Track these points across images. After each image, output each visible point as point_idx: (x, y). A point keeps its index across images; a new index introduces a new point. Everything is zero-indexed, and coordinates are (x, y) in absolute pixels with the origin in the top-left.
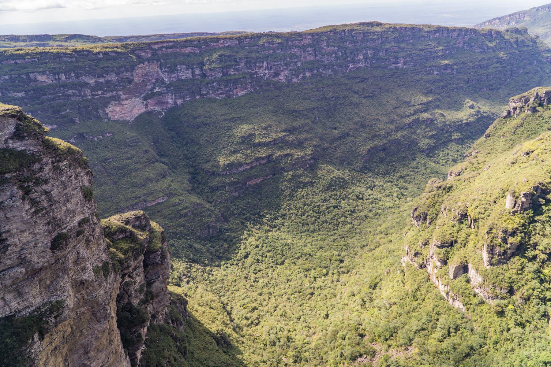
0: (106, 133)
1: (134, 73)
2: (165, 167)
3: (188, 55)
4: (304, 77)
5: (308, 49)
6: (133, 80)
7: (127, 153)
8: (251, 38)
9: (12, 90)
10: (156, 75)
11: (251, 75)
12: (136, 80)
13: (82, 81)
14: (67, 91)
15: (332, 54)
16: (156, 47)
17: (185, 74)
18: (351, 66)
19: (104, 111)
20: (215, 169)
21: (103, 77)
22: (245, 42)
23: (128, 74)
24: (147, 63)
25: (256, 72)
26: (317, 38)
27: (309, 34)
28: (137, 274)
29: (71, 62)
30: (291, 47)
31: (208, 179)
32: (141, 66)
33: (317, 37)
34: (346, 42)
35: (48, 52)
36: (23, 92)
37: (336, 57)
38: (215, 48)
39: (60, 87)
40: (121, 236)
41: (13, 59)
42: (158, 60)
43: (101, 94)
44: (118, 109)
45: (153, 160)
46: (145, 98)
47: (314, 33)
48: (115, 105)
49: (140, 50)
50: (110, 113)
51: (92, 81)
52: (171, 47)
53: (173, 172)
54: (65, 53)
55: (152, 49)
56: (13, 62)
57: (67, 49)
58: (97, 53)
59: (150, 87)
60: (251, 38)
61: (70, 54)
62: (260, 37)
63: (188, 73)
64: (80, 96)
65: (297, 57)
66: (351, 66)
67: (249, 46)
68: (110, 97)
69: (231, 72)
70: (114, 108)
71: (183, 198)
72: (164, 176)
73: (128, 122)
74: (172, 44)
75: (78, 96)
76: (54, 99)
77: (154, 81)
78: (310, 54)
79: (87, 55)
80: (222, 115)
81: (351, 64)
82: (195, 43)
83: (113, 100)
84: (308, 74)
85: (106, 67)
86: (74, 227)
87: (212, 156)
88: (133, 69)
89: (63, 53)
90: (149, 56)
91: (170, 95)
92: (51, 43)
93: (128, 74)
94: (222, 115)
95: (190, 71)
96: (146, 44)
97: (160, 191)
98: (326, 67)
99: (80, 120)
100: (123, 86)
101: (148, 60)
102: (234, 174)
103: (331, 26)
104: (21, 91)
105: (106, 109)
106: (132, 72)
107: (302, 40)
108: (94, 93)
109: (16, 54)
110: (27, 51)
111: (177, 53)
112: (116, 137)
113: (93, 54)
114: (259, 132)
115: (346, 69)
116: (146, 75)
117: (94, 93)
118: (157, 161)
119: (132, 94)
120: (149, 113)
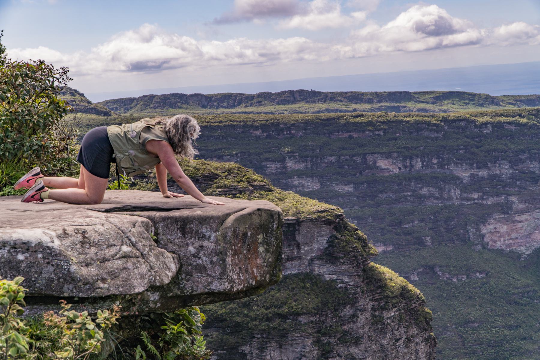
0: (475, 272)
7: (509, 315)
9: (337, 180)
13: (448, 172)
14: (421, 188)
19: (478, 229)
21: (486, 167)
29: (436, 139)
35: (402, 121)
36: (352, 185)
43: (478, 199)
44: (504, 228)
48: (500, 221)
50: (488, 235)
51: (465, 174)
54: (429, 123)
56: (346, 135)
57: (433, 116)
58: (483, 124)
61: (437, 125)
64: (441, 198)
68: (493, 205)
70: (497, 226)
73: (519, 256)
75: (437, 198)
76: (397, 200)
79: (464, 128)
85: (494, 150)
89: (425, 122)
92: (410, 105)
99: (433, 243)
100: (520, 187)
104: (348, 183)
108: (465, 195)
109: (354, 123)
110: (370, 119)
112: (492, 282)
117: (465, 195)
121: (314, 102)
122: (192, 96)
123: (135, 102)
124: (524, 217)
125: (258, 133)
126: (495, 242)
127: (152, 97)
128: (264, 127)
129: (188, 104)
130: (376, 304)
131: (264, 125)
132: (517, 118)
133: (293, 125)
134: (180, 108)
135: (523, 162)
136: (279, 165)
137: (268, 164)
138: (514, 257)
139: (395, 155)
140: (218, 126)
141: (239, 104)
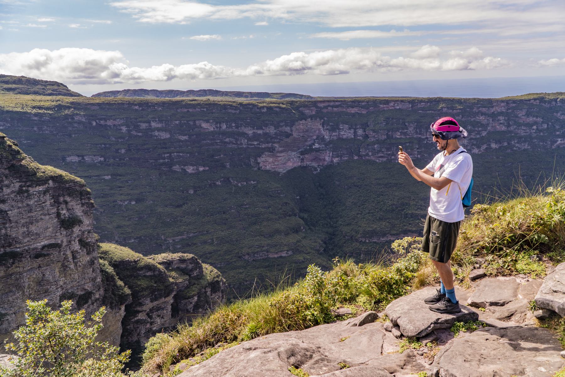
0: (250, 181)
1: (294, 128)
2: (302, 222)
3: (353, 115)
4: (489, 149)
5: (499, 117)
6: (291, 135)
7: (266, 202)
8: (428, 102)
9: (178, 133)
10: (317, 131)
11: (420, 140)
12: (295, 135)
13: (241, 131)
14: (225, 139)
15: (533, 126)
16: (322, 105)
17: (346, 133)
18: (559, 141)
19: (256, 160)
20: (354, 233)
21: (262, 129)
22: (419, 106)
23: (287, 129)
24: (309, 120)
25: (427, 138)
26: (513, 106)
27: (502, 101)
28: (159, 316)
30: (477, 114)
31: (345, 243)
32: (303, 121)
33: (514, 105)
34: (557, 112)
35: (217, 104)
37: (537, 129)
38: (384, 110)
39: (219, 134)
40: (149, 274)
42: (321, 118)
44: (271, 160)
45: (291, 213)
46: (302, 153)
47: (510, 100)
48: (269, 156)
51: (250, 132)
52: (337, 107)
53: (310, 229)
54: (231, 106)
55: (317, 107)
56: (186, 110)
58: (261, 107)
59: (310, 143)
60: (428, 102)
61: (236, 107)
63: (350, 133)
64: (237, 144)
65: (482, 125)
66: (559, 142)
67: (423, 110)
69: (398, 135)
70: (267, 158)
71: (309, 257)
72: (296, 230)
73: (279, 173)
75: (234, 144)
76: (212, 144)
77: (315, 137)
78: (501, 124)
80: (376, 179)
81: (559, 139)
82: (363, 104)
83: (267, 151)
84: (494, 146)
86: (36, 248)
87: (354, 219)
88: (294, 125)
89: (229, 105)
90: (314, 113)
91: (328, 152)
92: (268, 100)
93: (287, 129)
94: (376, 179)
95: (352, 131)
96: (312, 102)
97: (285, 245)
98: (520, 139)
99: (230, 166)
100: (280, 139)
101: (311, 117)
102: (375, 242)
103: (537, 94)
104: (185, 135)
105: (259, 159)
106: (291, 126)
107: (493, 107)
109: (190, 104)
111: (342, 112)
112: (259, 186)
113: (258, 108)
114: (415, 203)
115: (552, 145)
116: (307, 131)
118: (295, 215)
119: (288, 148)
120: (304, 168)
121: (216, 96)
122: (151, 90)
124: (282, 154)
125: (137, 107)
126: (266, 166)
127: (129, 90)
128: (141, 104)
129: (148, 94)
130: (23, 184)
131: (140, 103)
132: (281, 105)
133: (156, 104)
135: (282, 126)
136: (147, 125)
137: (141, 124)
138: (277, 174)
139: (211, 121)
141: (177, 96)
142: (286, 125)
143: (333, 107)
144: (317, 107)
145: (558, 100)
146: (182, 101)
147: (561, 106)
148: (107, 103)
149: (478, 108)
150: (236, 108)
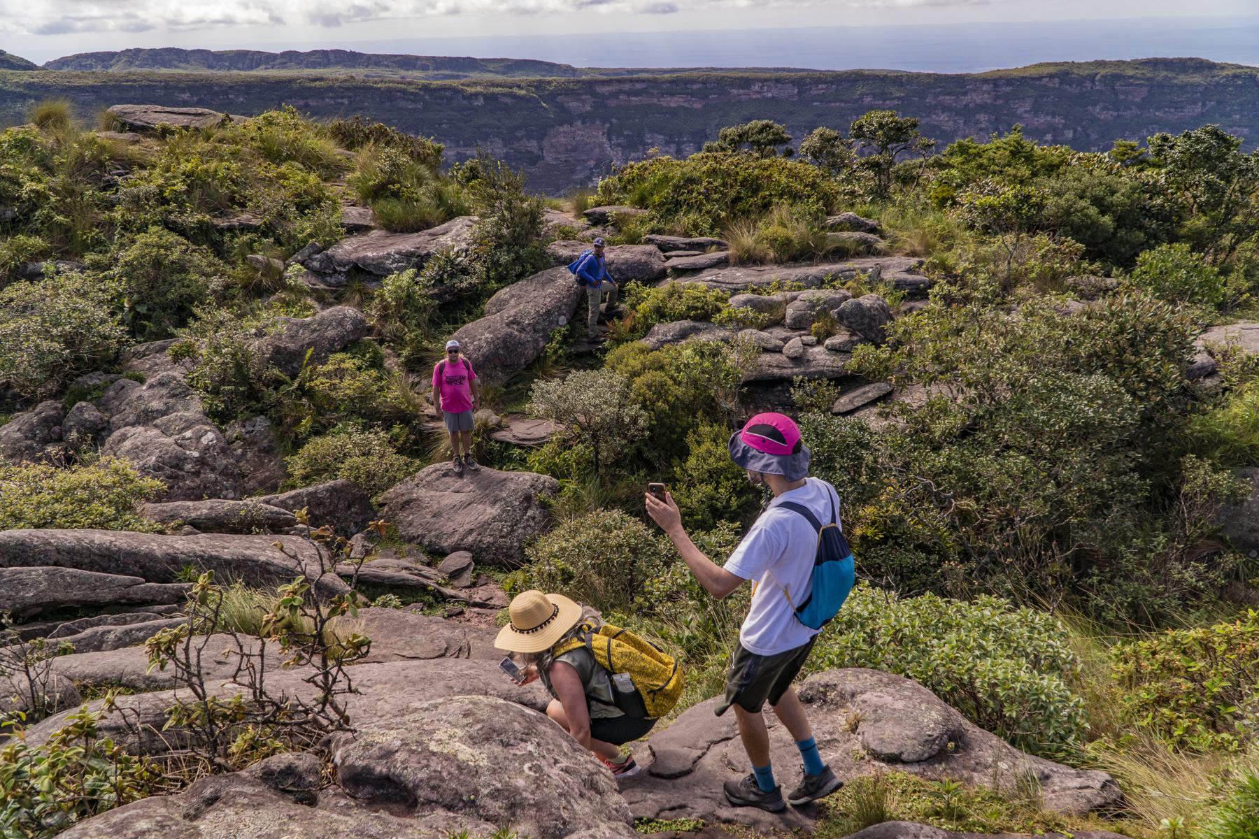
1: (545, 144)
3: (674, 113)
5: (978, 116)
6: (541, 158)
8: (832, 83)
12: (549, 158)
16: (605, 90)
22: (814, 92)
23: (532, 145)
24: (579, 123)
27: (984, 80)
29: (414, 110)
32: (566, 128)
33: (1009, 89)
34: (1094, 105)
35: (371, 88)
38: (740, 101)
41: (302, 98)
47: (1001, 78)
49: (566, 94)
54: (404, 92)
55: (595, 95)
57: (410, 83)
59: (581, 176)
61: (415, 95)
62: (855, 81)
67: (821, 101)
74: (643, 86)
77: (592, 163)
78: (981, 129)
79: (450, 99)
82: (695, 87)
88: (545, 135)
89: (400, 90)
92: (475, 76)
93: (532, 145)
96: (584, 82)
101: (584, 117)
103: (1056, 64)
106: (540, 138)
107: (965, 93)
109: (310, 88)
113: (464, 98)
116: (575, 149)
121: (354, 67)
122: (194, 52)
123: (116, 58)
127: (138, 51)
129: (188, 62)
132: (516, 90)
133: (231, 87)
134: (177, 67)
135: (520, 139)
140: (131, 86)
141: (258, 65)
142: (529, 137)
143: (629, 93)
144: (595, 95)
145: (1098, 77)
146: (292, 81)
147: (1101, 92)
148: (114, 86)
149: (936, 95)
150: (415, 97)
